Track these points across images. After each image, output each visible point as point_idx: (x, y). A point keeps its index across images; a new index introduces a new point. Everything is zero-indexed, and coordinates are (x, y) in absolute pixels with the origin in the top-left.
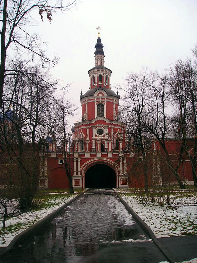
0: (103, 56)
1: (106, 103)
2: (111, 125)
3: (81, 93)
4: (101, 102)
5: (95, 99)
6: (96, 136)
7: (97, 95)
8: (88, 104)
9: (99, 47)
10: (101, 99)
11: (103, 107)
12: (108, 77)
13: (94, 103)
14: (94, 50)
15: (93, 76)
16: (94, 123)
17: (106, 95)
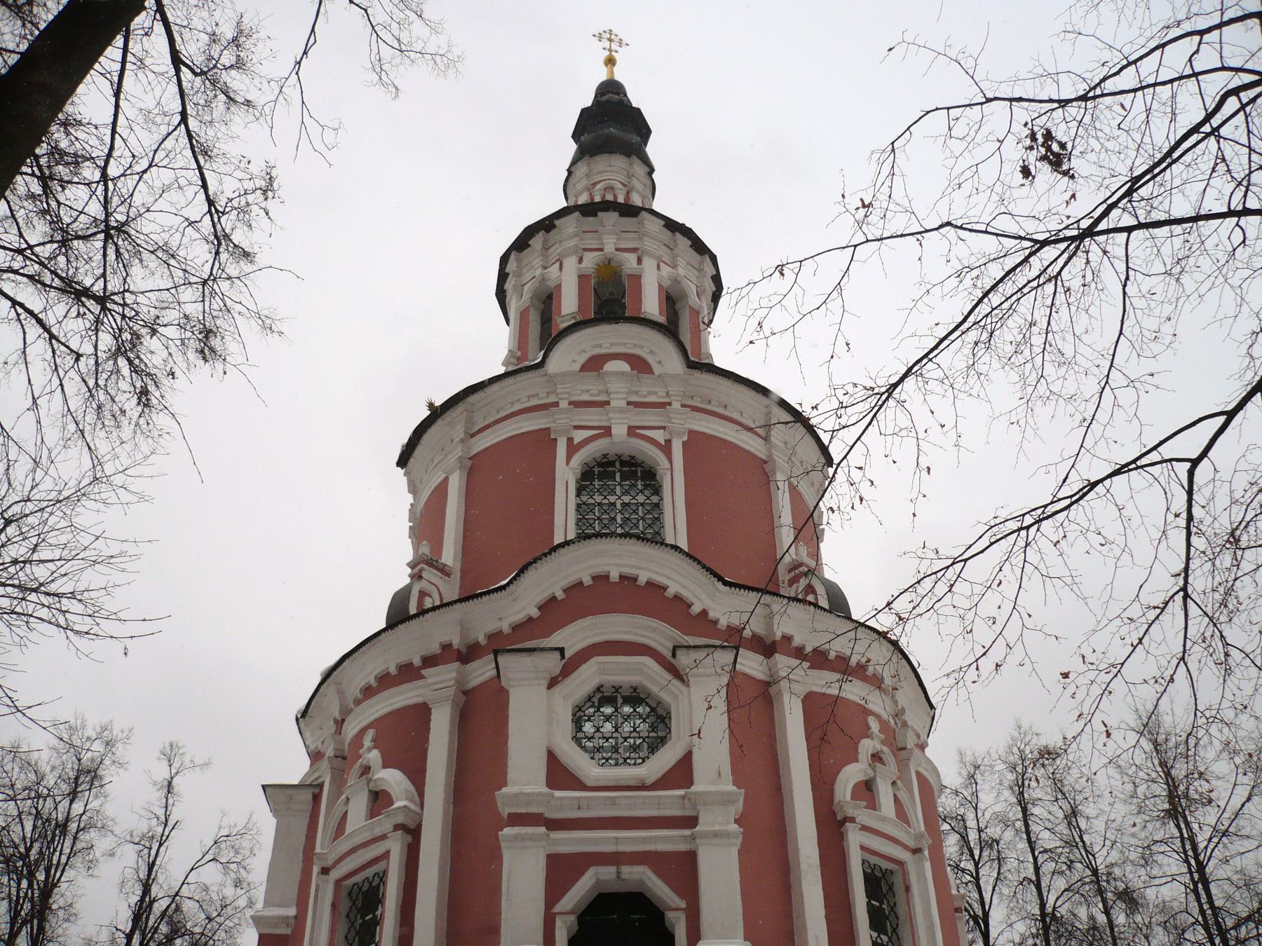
0: (639, 169)
2: (767, 648)
4: (632, 431)
6: (559, 775)
7: (577, 367)
8: (475, 468)
10: (623, 404)
11: (657, 491)
16: (535, 613)
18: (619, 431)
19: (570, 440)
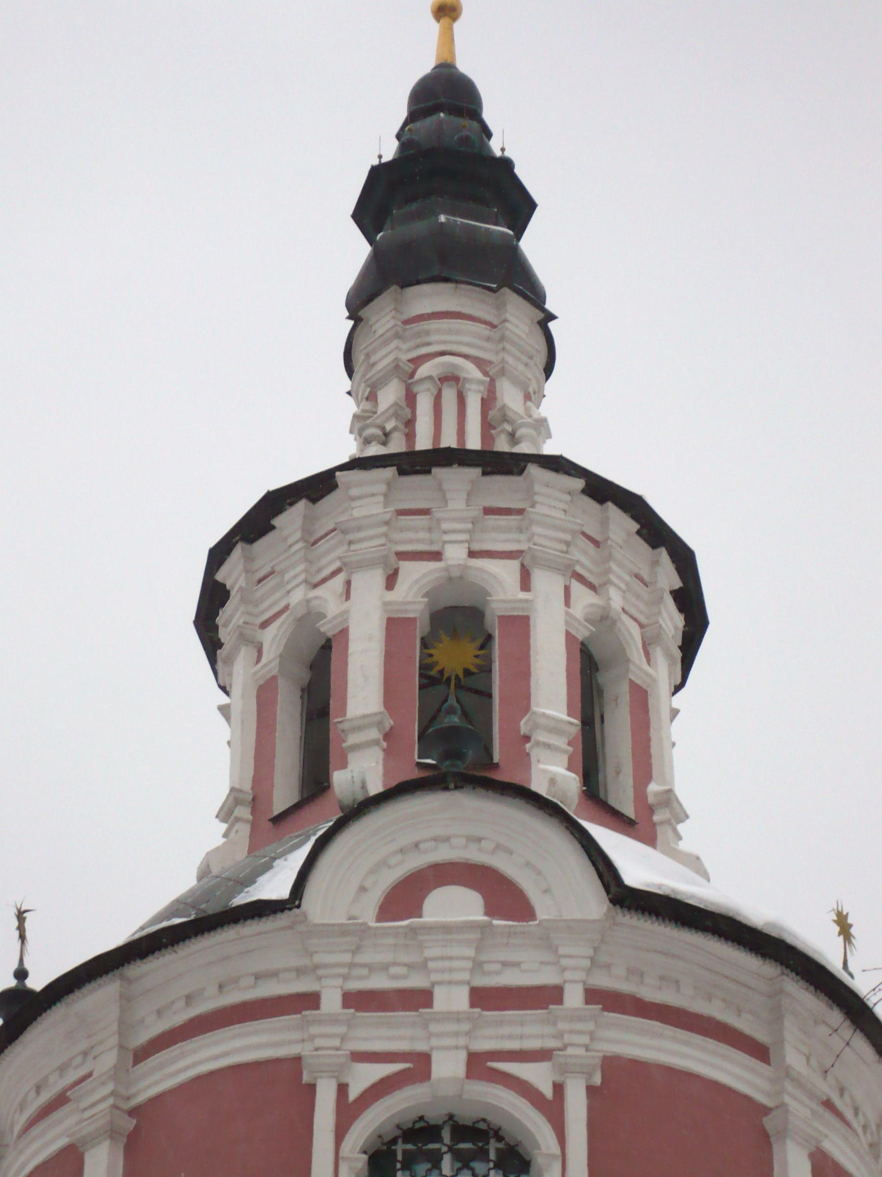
1: (591, 1090)
3: (21, 974)
4: (479, 1065)
5: (311, 1000)
9: (444, 204)
12: (636, 654)
13: (283, 1086)
14: (356, 251)
15: (310, 617)
17: (592, 902)
18: (448, 1067)
19: (342, 1089)
